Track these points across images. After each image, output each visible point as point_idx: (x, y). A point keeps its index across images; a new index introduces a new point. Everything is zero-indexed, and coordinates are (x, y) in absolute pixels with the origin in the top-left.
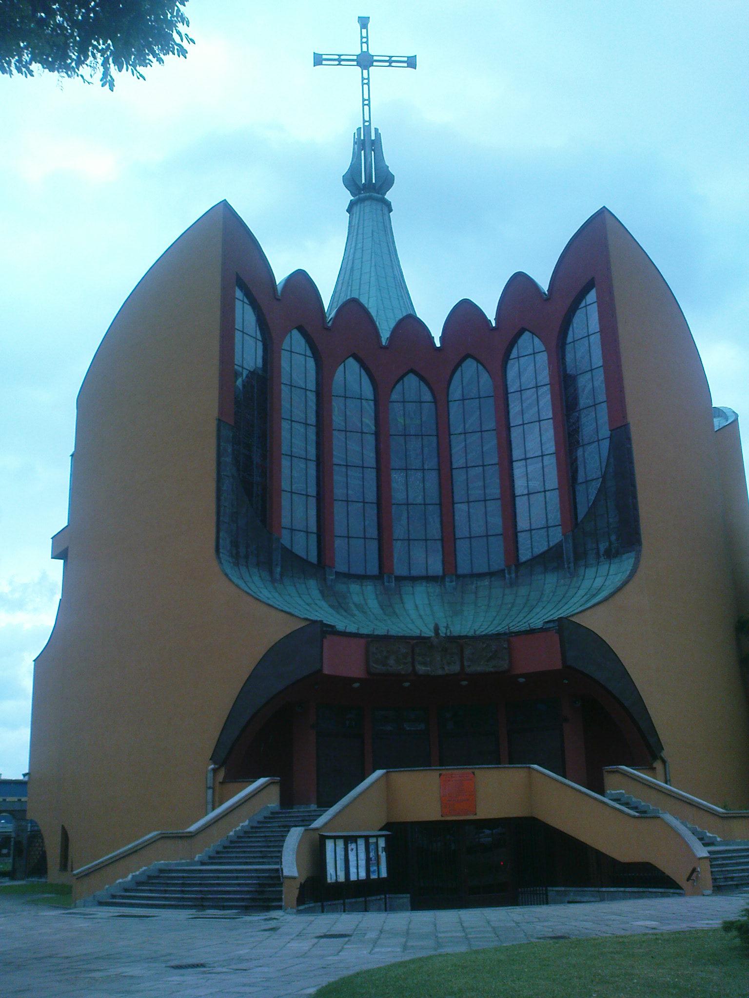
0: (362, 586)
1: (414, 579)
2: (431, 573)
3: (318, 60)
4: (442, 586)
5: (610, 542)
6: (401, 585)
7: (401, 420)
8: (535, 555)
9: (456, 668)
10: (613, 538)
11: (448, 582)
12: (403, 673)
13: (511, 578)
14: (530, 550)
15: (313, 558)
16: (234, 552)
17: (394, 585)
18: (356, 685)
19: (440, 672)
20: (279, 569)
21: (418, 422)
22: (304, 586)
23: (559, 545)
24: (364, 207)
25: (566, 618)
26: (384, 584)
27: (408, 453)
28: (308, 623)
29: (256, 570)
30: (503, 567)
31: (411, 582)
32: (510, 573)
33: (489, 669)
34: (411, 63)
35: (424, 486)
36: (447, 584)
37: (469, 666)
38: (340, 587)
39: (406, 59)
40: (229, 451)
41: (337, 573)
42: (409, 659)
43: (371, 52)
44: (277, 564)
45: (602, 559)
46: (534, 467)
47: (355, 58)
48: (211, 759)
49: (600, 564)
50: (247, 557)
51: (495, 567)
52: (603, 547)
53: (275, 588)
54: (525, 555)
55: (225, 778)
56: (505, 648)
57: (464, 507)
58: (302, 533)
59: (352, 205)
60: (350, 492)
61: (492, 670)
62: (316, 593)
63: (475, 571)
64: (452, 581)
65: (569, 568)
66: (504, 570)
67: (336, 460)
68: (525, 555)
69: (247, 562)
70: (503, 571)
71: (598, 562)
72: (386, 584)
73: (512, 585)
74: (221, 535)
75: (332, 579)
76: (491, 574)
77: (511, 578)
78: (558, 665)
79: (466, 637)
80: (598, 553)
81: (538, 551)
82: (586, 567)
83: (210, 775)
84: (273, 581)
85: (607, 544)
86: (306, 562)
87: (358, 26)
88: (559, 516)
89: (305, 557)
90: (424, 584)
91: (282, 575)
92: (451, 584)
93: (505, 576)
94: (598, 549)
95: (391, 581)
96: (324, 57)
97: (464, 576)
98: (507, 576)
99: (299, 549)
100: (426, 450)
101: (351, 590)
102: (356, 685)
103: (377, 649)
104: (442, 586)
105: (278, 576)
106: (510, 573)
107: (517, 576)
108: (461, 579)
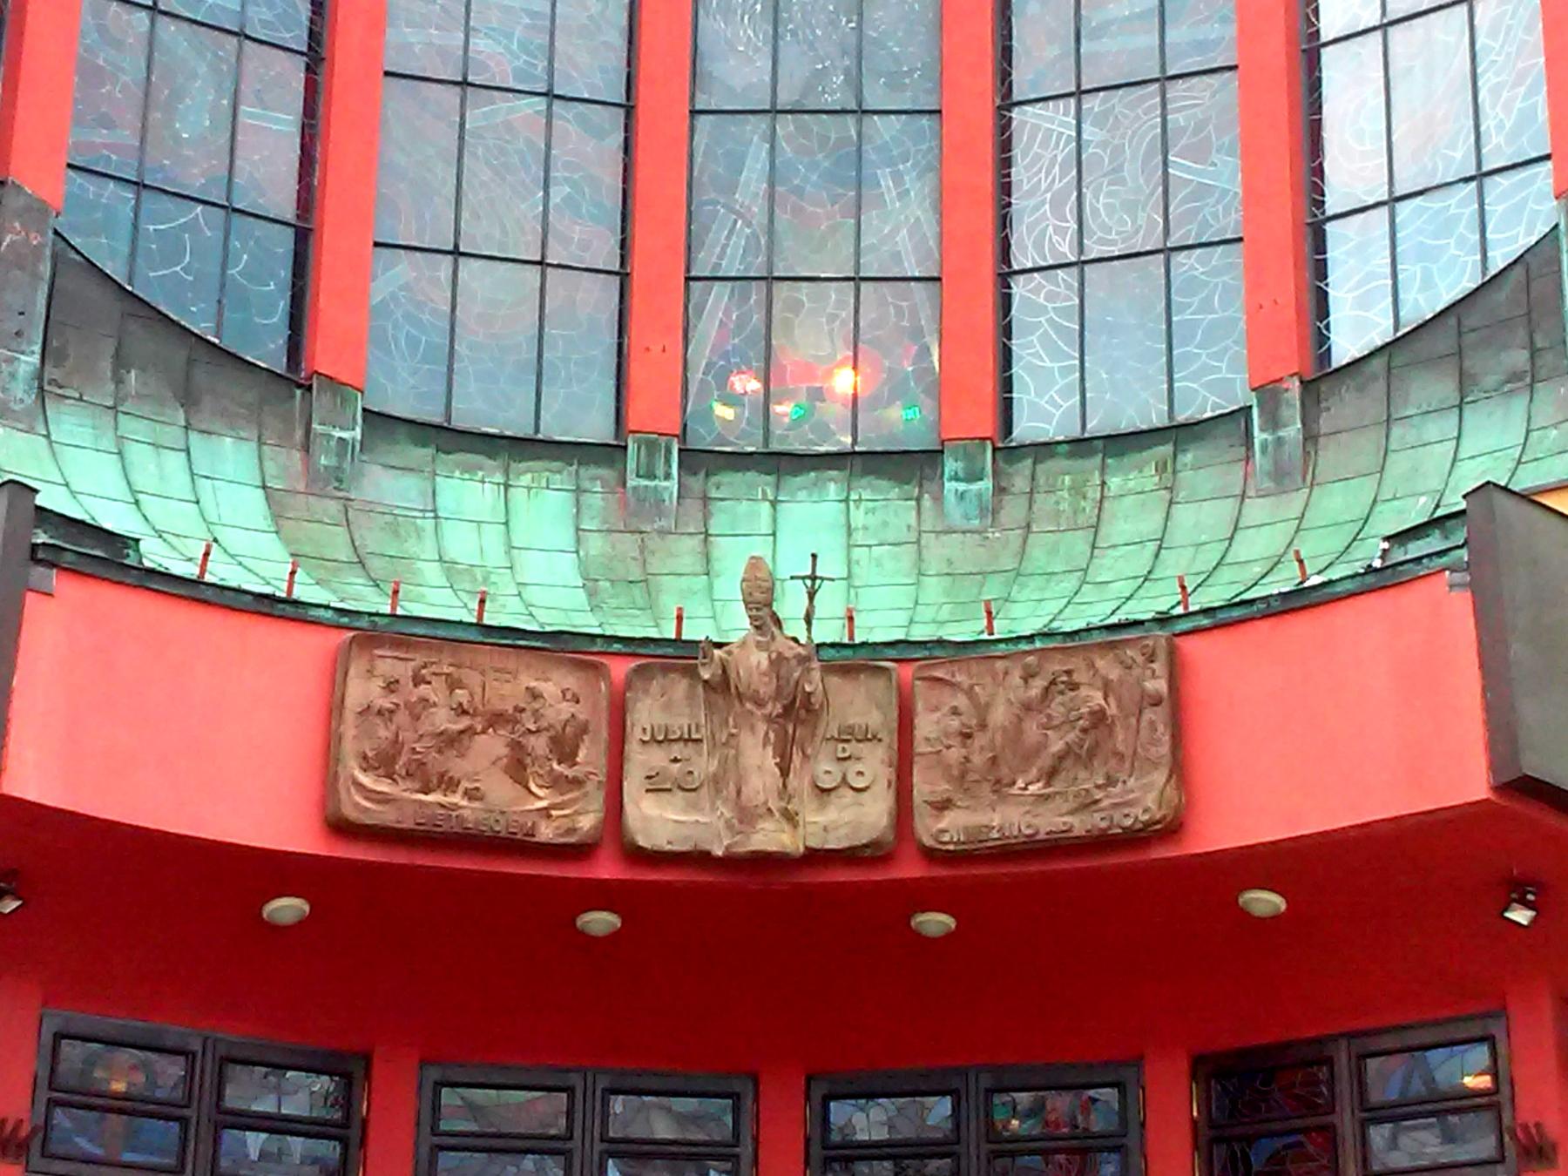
4: (927, 501)
6: (714, 494)
11: (956, 478)
12: (546, 833)
15: (269, 352)
17: (673, 485)
18: (286, 908)
19: (771, 837)
22: (176, 461)
25: (1526, 497)
30: (1242, 395)
31: (771, 479)
32: (1273, 422)
33: (1052, 820)
35: (859, 28)
36: (950, 486)
37: (943, 806)
42: (592, 756)
51: (1200, 403)
56: (1157, 702)
57: (1058, 118)
60: (479, 44)
61: (1080, 825)
63: (1095, 426)
64: (973, 476)
72: (632, 482)
73: (1281, 479)
75: (340, 438)
76: (1180, 433)
77: (1279, 442)
81: (1421, 304)
88: (1543, 115)
90: (833, 490)
92: (975, 486)
95: (660, 471)
97: (1043, 450)
98: (1259, 436)
101: (445, 502)
102: (286, 908)
103: (391, 686)
104: (927, 501)
106: (1273, 422)
107: (1311, 437)
108: (1029, 462)
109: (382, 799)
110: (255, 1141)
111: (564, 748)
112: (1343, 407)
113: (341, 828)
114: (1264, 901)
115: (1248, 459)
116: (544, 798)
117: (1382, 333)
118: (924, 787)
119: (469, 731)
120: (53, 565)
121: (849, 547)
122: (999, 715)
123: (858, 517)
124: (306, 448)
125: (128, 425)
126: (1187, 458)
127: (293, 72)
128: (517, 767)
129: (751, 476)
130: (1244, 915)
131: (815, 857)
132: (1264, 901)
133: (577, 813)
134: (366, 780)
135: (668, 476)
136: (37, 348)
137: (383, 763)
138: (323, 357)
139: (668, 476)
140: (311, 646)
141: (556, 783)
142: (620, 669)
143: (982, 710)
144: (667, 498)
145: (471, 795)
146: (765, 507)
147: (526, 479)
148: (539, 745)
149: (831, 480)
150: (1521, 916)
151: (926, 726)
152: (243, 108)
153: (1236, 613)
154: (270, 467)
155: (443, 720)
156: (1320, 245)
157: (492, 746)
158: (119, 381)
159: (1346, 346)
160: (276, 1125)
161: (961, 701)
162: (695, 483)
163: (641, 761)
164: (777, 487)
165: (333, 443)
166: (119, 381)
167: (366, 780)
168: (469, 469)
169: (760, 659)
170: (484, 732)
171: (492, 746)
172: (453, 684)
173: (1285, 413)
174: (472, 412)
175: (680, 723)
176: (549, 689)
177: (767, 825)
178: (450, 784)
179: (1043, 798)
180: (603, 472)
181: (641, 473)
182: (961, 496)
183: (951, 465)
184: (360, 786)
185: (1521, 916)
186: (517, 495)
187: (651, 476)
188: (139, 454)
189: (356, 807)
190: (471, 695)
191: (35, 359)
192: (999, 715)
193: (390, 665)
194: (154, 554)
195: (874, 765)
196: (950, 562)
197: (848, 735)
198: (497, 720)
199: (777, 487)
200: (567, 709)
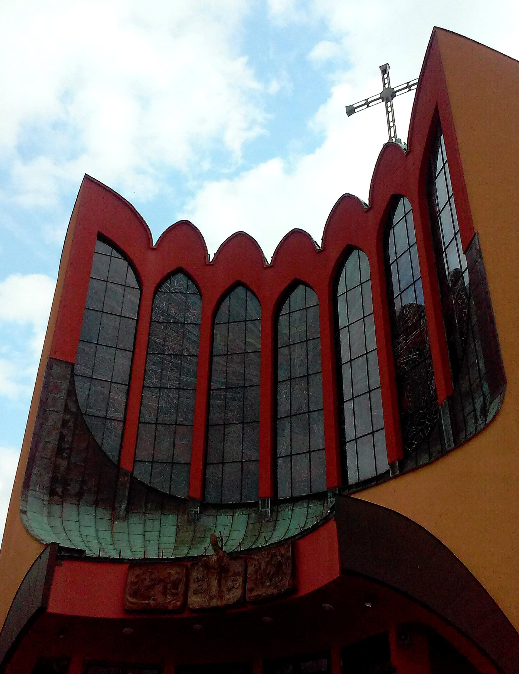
2: (315, 490)
3: (351, 111)
4: (326, 504)
9: (234, 596)
11: (331, 498)
16: (59, 490)
19: (215, 602)
20: (124, 506)
21: (303, 328)
22: (157, 523)
27: (292, 362)
29: (91, 510)
31: (292, 504)
36: (329, 500)
37: (252, 590)
42: (181, 587)
44: (122, 501)
47: (379, 96)
66: (389, 470)
70: (388, 472)
75: (195, 511)
87: (380, 72)
95: (266, 507)
100: (311, 355)
103: (137, 576)
105: (122, 513)
111: (175, 585)
113: (127, 611)
116: (169, 598)
118: (249, 585)
119: (154, 585)
122: (263, 565)
123: (310, 511)
131: (228, 607)
133: (176, 602)
134: (130, 599)
135: (268, 507)
136: (126, 503)
137: (134, 595)
141: (173, 595)
142: (189, 564)
143: (260, 564)
144: (268, 513)
145: (153, 600)
146: (290, 512)
148: (169, 586)
150: (368, 605)
151: (251, 569)
153: (306, 533)
154: (180, 520)
155: (147, 582)
158: (146, 506)
162: (275, 508)
163: (193, 586)
164: (293, 506)
165: (193, 512)
166: (146, 506)
167: (130, 599)
168: (225, 513)
169: (215, 558)
170: (157, 584)
171: (159, 587)
172: (151, 574)
175: (201, 576)
177: (215, 600)
178: (149, 598)
179: (269, 586)
181: (262, 507)
183: (330, 494)
185: (368, 605)
186: (236, 517)
188: (149, 523)
190: (155, 576)
191: (126, 505)
192: (263, 565)
193: (138, 571)
194: (89, 553)
195: (240, 580)
198: (161, 581)
199: (293, 506)
200: (176, 576)
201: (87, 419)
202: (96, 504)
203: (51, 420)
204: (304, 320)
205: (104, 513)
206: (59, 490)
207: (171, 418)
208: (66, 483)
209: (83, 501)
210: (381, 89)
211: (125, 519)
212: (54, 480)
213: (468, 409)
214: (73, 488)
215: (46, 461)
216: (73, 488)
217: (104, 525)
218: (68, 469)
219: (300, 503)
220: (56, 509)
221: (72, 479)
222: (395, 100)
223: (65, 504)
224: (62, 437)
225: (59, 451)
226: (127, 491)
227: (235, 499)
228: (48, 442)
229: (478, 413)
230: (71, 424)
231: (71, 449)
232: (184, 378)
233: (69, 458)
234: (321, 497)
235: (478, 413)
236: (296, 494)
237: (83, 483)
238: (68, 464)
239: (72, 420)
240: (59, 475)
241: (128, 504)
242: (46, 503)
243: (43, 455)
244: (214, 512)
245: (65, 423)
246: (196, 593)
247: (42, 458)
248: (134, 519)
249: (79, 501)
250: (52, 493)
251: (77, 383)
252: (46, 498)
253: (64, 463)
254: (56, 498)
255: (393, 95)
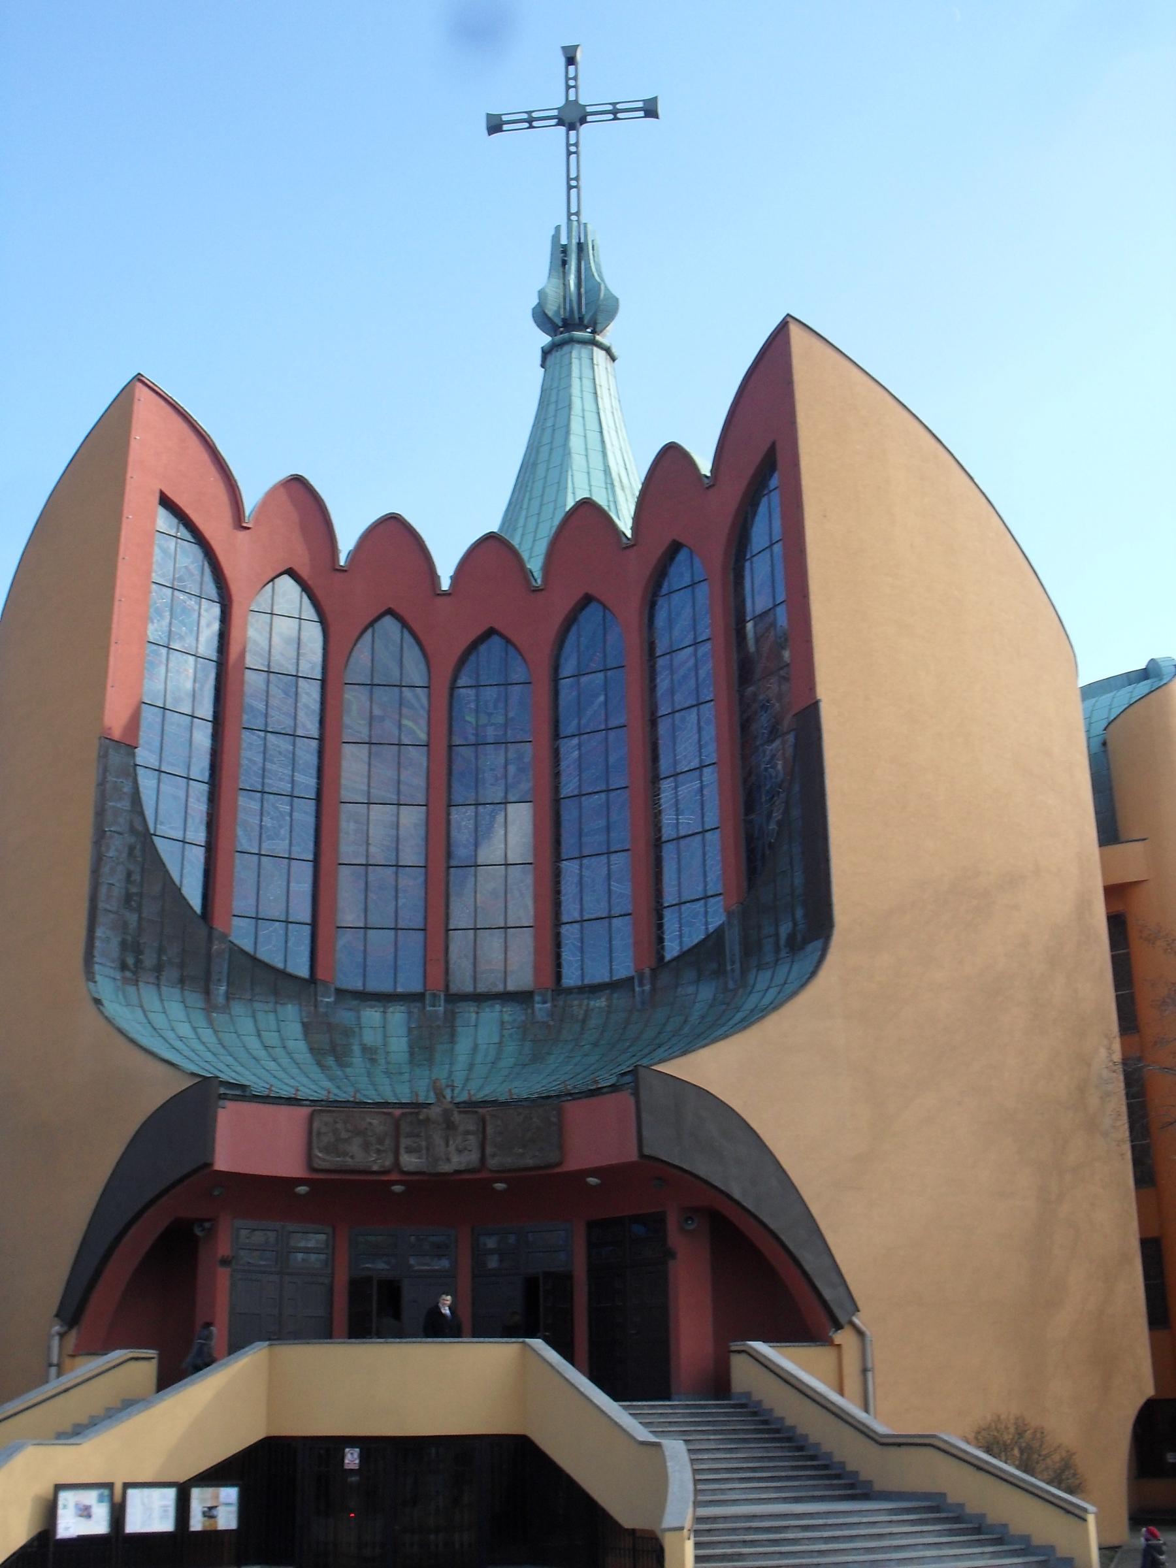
0: (385, 1012)
1: (480, 998)
3: (495, 126)
5: (795, 924)
7: (470, 718)
8: (685, 948)
10: (799, 913)
11: (538, 1003)
12: (375, 1168)
13: (643, 991)
14: (678, 941)
16: (130, 961)
17: (441, 1009)
20: (223, 988)
21: (500, 719)
22: (272, 1016)
23: (720, 931)
24: (562, 356)
26: (424, 1007)
28: (198, 1080)
29: (176, 992)
31: (475, 1004)
32: (641, 984)
34: (650, 110)
36: (538, 1006)
37: (494, 1155)
38: (344, 1016)
39: (640, 105)
40: (125, 790)
41: (340, 993)
42: (388, 1142)
43: (582, 102)
44: (219, 980)
45: (783, 954)
46: (688, 788)
47: (555, 113)
48: (57, 1315)
49: (779, 962)
50: (158, 969)
52: (785, 929)
53: (211, 1023)
54: (672, 950)
55: (77, 1346)
58: (278, 923)
59: (546, 353)
62: (294, 1028)
64: (545, 1002)
65: (733, 970)
67: (345, 795)
68: (672, 950)
69: (158, 978)
70: (631, 979)
71: (777, 960)
72: (428, 1008)
74: (99, 932)
75: (327, 1002)
77: (643, 991)
78: (633, 1156)
79: (495, 1103)
80: (777, 944)
82: (760, 967)
83: (56, 1342)
84: (210, 1007)
85: (790, 924)
86: (284, 975)
87: (562, 61)
89: (280, 966)
90: (498, 1007)
91: (228, 997)
92: (546, 1005)
93: (634, 990)
94: (777, 935)
95: (437, 1004)
96: (505, 118)
97: (569, 991)
98: (637, 989)
99: (270, 953)
100: (512, 769)
101: (364, 1020)
105: (221, 1000)
106: (641, 984)
107: (654, 989)
109: (324, 1160)
110: (300, 1256)
111: (380, 1141)
112: (665, 978)
114: (592, 1180)
115: (634, 997)
116: (374, 1156)
117: (675, 953)
118: (489, 1150)
120: (225, 1099)
121: (502, 1029)
124: (316, 1006)
125: (257, 1005)
126: (616, 995)
127: (308, 868)
128: (366, 1147)
129: (471, 1003)
130: (586, 1183)
131: (457, 1172)
132: (592, 1180)
134: (320, 1155)
136: (225, 984)
137: (326, 1149)
138: (320, 975)
139: (440, 1006)
140: (304, 1111)
141: (378, 1151)
145: (352, 1157)
147: (391, 1009)
149: (497, 1004)
152: (292, 885)
156: (660, 917)
157: (358, 1141)
159: (668, 957)
160: (307, 1251)
161: (499, 1122)
163: (404, 1142)
166: (252, 989)
167: (320, 1155)
168: (372, 1007)
171: (358, 1141)
173: (645, 982)
174: (373, 986)
176: (375, 1122)
178: (345, 1154)
180: (419, 1005)
182: (540, 1009)
183: (537, 998)
184: (319, 1157)
186: (389, 1015)
187: (434, 1006)
188: (260, 1016)
189: (317, 1164)
193: (327, 1118)
196: (535, 1035)
197: (467, 1133)
201: (156, 840)
202: (182, 981)
203: (113, 848)
204: (501, 705)
205: (195, 999)
206: (130, 961)
207: (280, 847)
208: (138, 950)
209: (163, 978)
210: (561, 102)
211: (226, 1009)
212: (123, 945)
213: (768, 930)
214: (149, 960)
215: (112, 916)
216: (149, 960)
217: (200, 1019)
218: (140, 928)
219: (490, 1003)
220: (131, 990)
221: (145, 943)
222: (584, 129)
223: (141, 984)
224: (129, 874)
225: (128, 898)
226: (226, 966)
227: (386, 987)
228: (113, 885)
229: (782, 942)
230: (137, 852)
231: (141, 895)
232: (299, 777)
233: (139, 910)
234: (522, 998)
235: (782, 942)
236: (482, 988)
237: (161, 951)
238: (140, 918)
239: (138, 847)
240: (129, 938)
241: (228, 986)
242: (119, 983)
243: (108, 907)
244: (355, 1003)
245: (131, 849)
246: (409, 1150)
247: (106, 910)
248: (238, 1008)
249: (158, 978)
250: (123, 967)
251: (140, 779)
252: (118, 975)
253: (133, 918)
254: (128, 974)
255: (583, 121)
